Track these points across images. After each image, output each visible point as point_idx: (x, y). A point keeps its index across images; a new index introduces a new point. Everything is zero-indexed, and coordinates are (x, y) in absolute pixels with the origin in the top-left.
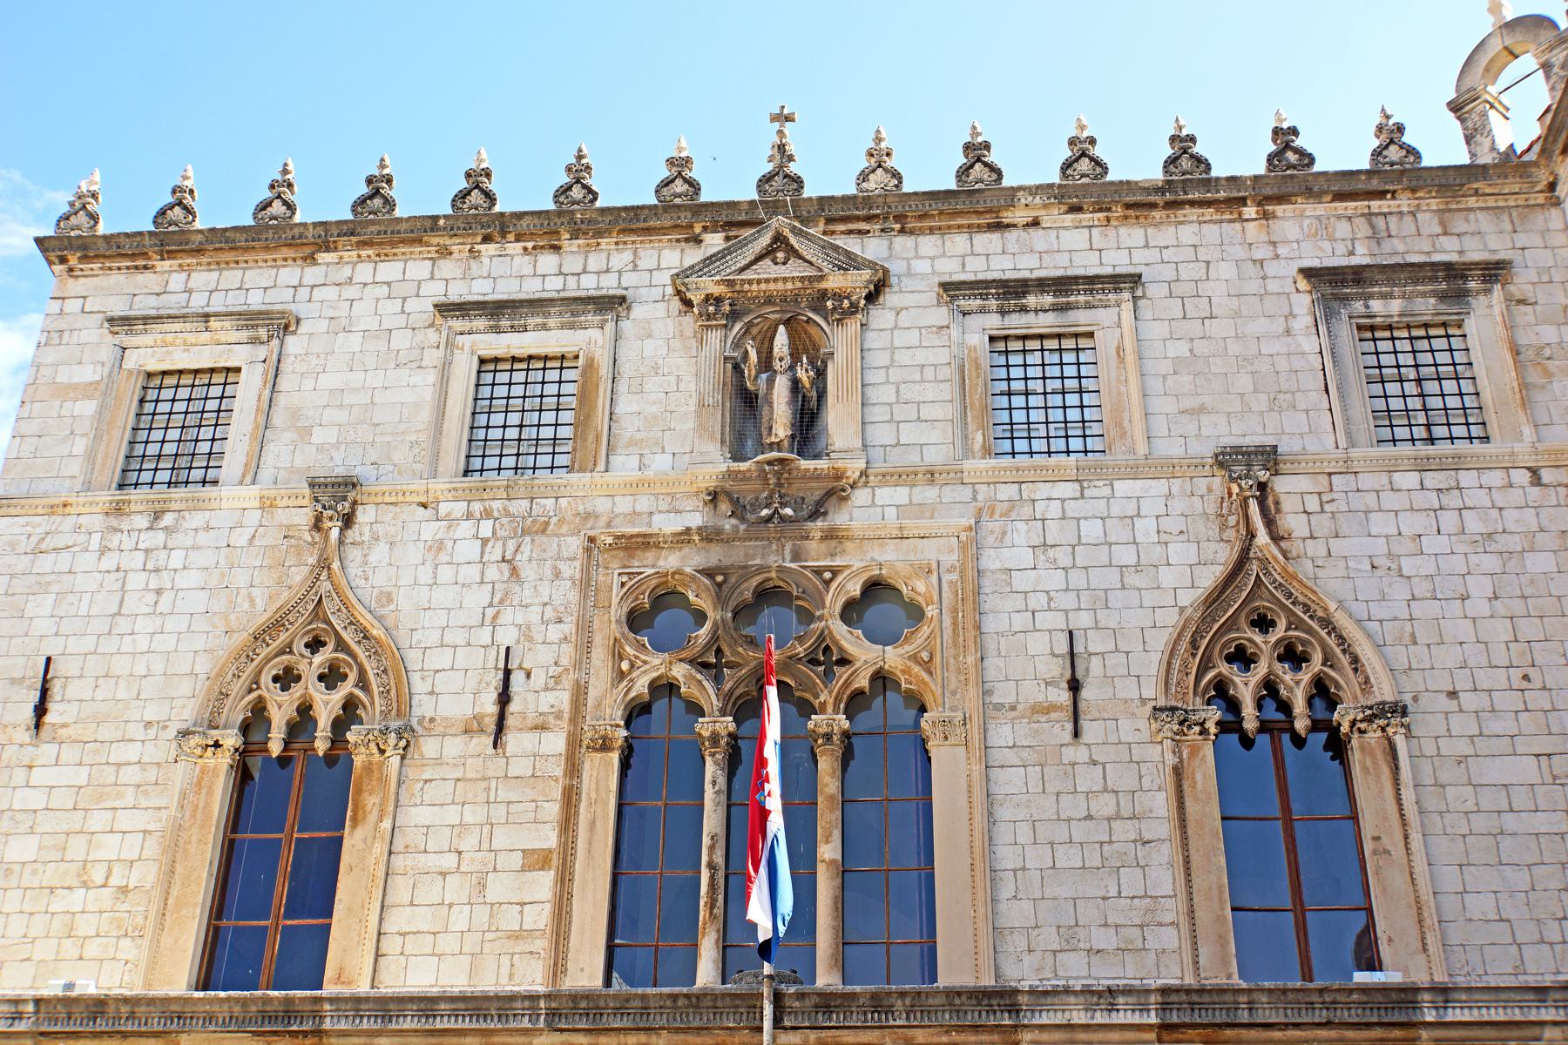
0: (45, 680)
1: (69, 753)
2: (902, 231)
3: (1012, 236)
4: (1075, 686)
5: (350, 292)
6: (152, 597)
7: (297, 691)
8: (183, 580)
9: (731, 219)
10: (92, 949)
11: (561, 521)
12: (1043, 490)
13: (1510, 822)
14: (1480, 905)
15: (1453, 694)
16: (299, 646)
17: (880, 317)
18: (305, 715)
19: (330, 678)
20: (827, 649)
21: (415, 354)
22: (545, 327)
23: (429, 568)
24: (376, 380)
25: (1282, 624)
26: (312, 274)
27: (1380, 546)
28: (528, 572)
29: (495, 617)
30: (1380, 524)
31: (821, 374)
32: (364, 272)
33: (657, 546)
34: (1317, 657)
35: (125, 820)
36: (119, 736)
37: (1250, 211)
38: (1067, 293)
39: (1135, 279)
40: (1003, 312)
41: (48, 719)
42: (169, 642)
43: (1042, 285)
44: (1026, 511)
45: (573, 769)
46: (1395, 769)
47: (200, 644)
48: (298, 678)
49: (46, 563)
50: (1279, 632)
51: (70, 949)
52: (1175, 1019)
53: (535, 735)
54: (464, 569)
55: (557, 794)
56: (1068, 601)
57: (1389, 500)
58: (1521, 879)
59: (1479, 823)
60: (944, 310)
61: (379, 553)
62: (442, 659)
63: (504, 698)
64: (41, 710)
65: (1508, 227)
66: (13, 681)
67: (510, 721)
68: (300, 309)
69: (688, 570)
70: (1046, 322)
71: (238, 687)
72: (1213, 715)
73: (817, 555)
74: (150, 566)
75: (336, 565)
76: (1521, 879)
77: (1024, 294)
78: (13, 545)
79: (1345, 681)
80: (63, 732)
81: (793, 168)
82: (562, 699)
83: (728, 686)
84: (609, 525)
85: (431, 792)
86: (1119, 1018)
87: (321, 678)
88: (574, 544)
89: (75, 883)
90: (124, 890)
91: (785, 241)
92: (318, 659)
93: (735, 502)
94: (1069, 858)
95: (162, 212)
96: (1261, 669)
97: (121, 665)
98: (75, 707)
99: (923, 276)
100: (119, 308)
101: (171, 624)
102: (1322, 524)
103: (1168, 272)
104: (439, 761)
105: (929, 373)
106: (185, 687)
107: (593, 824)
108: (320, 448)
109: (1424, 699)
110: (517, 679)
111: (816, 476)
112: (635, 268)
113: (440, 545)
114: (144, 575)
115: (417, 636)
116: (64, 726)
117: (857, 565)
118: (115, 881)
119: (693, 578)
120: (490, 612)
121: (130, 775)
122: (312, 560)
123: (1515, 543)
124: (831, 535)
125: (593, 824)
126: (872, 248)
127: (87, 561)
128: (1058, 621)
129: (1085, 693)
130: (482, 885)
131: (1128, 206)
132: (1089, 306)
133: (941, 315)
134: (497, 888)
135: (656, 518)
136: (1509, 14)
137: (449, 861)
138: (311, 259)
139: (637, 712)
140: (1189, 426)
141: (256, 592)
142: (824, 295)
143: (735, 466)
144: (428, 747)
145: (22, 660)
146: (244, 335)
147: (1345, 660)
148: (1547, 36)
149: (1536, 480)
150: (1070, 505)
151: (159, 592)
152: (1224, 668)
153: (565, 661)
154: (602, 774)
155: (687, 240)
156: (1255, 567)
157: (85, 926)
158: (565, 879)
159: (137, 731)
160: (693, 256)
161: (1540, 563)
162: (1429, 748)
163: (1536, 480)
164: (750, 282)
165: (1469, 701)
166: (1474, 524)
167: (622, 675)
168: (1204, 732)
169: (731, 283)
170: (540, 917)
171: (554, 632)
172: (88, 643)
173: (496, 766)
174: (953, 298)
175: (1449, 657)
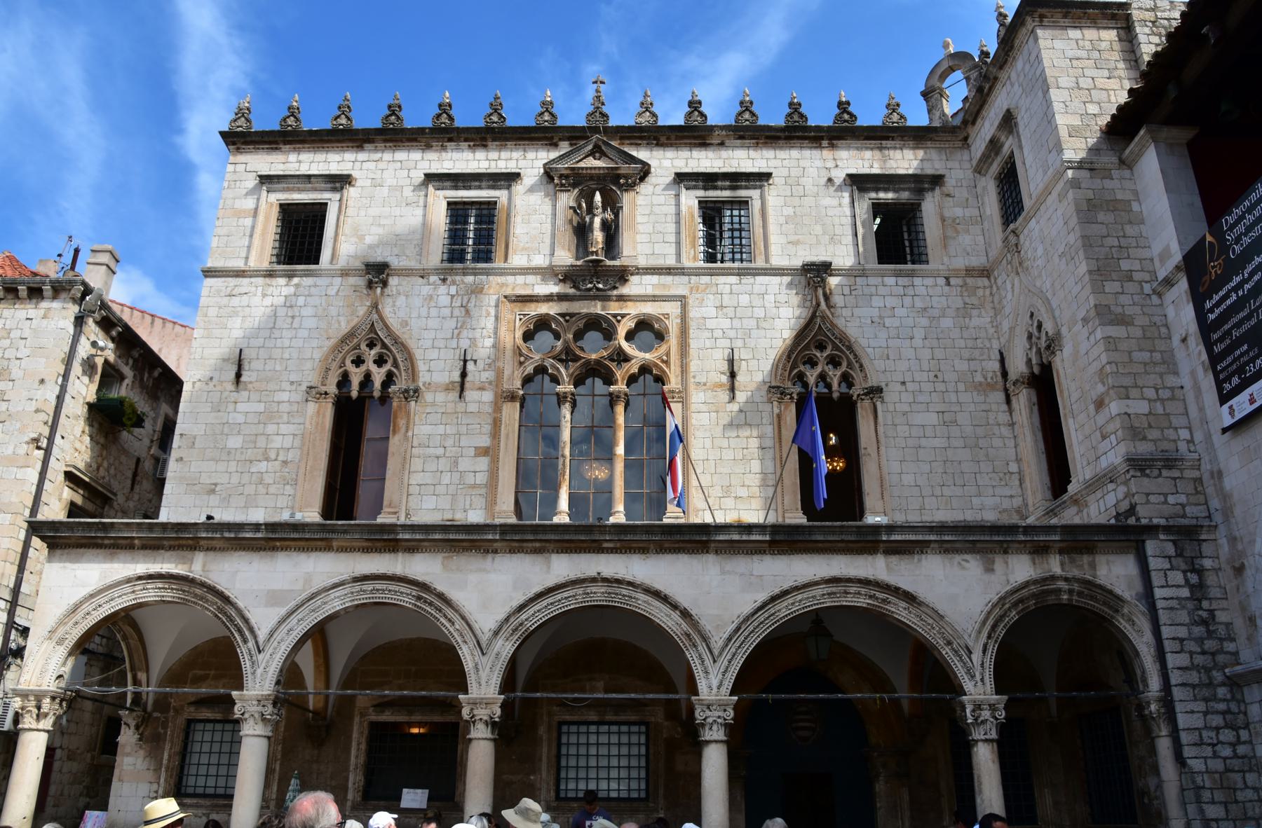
0: (240, 360)
1: (254, 396)
2: (657, 145)
4: (733, 375)
5: (381, 165)
6: (289, 320)
7: (363, 368)
8: (305, 312)
9: (575, 135)
10: (272, 490)
12: (722, 279)
13: (924, 442)
14: (908, 479)
15: (903, 383)
16: (363, 346)
17: (644, 188)
18: (368, 377)
19: (380, 361)
22: (480, 188)
23: (425, 309)
24: (397, 211)
25: (830, 347)
26: (362, 156)
27: (875, 313)
30: (877, 302)
31: (617, 215)
32: (387, 156)
33: (537, 301)
34: (845, 364)
35: (284, 429)
37: (825, 143)
38: (737, 181)
39: (768, 176)
40: (705, 189)
41: (243, 379)
42: (299, 343)
43: (726, 176)
44: (714, 289)
45: (497, 409)
46: (876, 417)
47: (315, 343)
48: (363, 362)
49: (235, 301)
50: (827, 352)
51: (262, 489)
52: (777, 538)
53: (479, 393)
55: (490, 421)
56: (732, 334)
57: (882, 290)
58: (926, 468)
59: (911, 442)
61: (401, 301)
62: (433, 354)
63: (464, 375)
64: (238, 375)
65: (944, 157)
67: (467, 385)
68: (355, 174)
71: (334, 365)
72: (798, 389)
73: (614, 308)
76: (926, 468)
77: (716, 180)
78: (219, 291)
79: (857, 376)
80: (250, 386)
81: (605, 109)
83: (571, 371)
85: (431, 418)
86: (753, 538)
87: (375, 362)
89: (260, 457)
90: (285, 462)
91: (600, 147)
92: (373, 352)
93: (574, 282)
94: (728, 455)
95: (285, 120)
96: (819, 369)
97: (277, 353)
99: (667, 168)
100: (265, 171)
102: (851, 300)
103: (785, 172)
104: (433, 404)
106: (309, 365)
107: (507, 435)
109: (891, 385)
110: (470, 366)
113: (431, 297)
115: (421, 343)
118: (280, 458)
119: (554, 318)
120: (456, 332)
121: (285, 407)
122: (368, 304)
123: (936, 313)
124: (622, 298)
125: (507, 435)
126: (642, 154)
127: (256, 300)
128: (727, 343)
129: (738, 378)
130: (456, 463)
131: (767, 137)
132: (747, 188)
134: (464, 464)
136: (952, 50)
138: (360, 147)
139: (527, 380)
140: (792, 249)
141: (341, 318)
142: (619, 176)
144: (428, 397)
146: (329, 186)
147: (857, 365)
148: (969, 64)
149: (948, 284)
150: (734, 287)
151: (293, 317)
152: (802, 368)
154: (511, 413)
156: (819, 320)
157: (268, 479)
158: (495, 462)
159: (286, 386)
160: (554, 154)
161: (947, 323)
162: (891, 408)
163: (948, 284)
165: (910, 386)
166: (919, 303)
167: (521, 363)
168: (792, 398)
169: (573, 169)
170: (481, 478)
173: (461, 407)
174: (681, 181)
175: (903, 365)
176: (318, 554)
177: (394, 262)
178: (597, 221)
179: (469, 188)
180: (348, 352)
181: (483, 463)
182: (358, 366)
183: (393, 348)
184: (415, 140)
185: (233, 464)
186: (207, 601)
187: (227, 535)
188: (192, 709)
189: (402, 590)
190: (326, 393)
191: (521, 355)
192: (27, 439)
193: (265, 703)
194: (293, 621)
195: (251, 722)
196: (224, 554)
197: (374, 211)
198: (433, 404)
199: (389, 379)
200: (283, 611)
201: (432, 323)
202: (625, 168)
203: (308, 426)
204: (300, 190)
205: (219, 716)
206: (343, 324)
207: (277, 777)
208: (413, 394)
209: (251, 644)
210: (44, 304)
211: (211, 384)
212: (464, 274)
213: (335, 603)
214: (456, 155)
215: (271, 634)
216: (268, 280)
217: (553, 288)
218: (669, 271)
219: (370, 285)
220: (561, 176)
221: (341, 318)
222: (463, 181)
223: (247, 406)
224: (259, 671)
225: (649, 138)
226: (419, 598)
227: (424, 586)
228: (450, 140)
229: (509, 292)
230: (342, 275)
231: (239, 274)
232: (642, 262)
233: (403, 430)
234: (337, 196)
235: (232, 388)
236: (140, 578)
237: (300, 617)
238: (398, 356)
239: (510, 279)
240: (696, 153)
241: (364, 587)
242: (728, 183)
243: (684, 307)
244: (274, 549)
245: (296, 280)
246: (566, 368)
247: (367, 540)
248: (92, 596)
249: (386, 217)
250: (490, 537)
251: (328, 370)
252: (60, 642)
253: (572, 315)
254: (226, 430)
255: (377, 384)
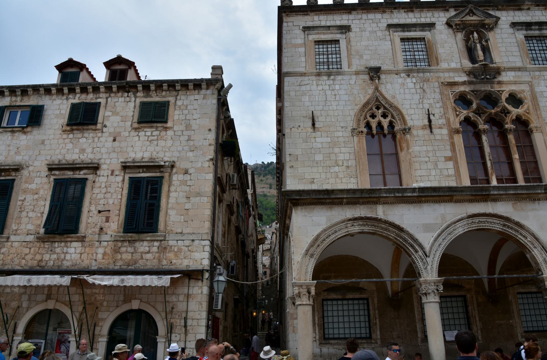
0: (313, 116)
1: (324, 134)
3: (524, 12)
5: (362, 21)
6: (334, 97)
7: (376, 119)
11: (432, 79)
16: (374, 109)
17: (497, 31)
18: (380, 124)
20: (504, 110)
21: (384, 37)
22: (415, 31)
26: (351, 17)
28: (428, 91)
29: (422, 102)
32: (364, 16)
33: (458, 85)
35: (343, 150)
36: (335, 130)
40: (526, 30)
41: (316, 126)
44: (543, 78)
45: (451, 138)
47: (350, 107)
48: (376, 116)
49: (303, 88)
54: (411, 90)
60: (512, 29)
61: (389, 86)
62: (412, 112)
63: (430, 121)
64: (313, 124)
66: (304, 117)
67: (433, 126)
69: (467, 90)
70: (537, 33)
71: (362, 118)
73: (497, 88)
74: (331, 89)
75: (380, 89)
77: (531, 26)
82: (443, 121)
84: (444, 79)
87: (382, 116)
88: (436, 84)
92: (380, 111)
97: (331, 113)
98: (322, 123)
101: (341, 103)
105: (512, 45)
106: (349, 118)
108: (366, 60)
110: (432, 117)
111: (493, 68)
112: (434, 17)
114: (330, 91)
115: (404, 106)
116: (321, 128)
117: (507, 90)
118: (345, 164)
119: (468, 93)
120: (421, 100)
124: (500, 83)
133: (511, 31)
134: (441, 165)
135: (455, 78)
137: (427, 159)
138: (350, 13)
141: (360, 95)
143: (474, 66)
144: (414, 132)
145: (305, 112)
146: (339, 31)
151: (335, 95)
153: (442, 112)
154: (459, 139)
155: (445, 10)
157: (341, 175)
158: (456, 163)
159: (339, 129)
164: (467, 21)
167: (457, 115)
169: (462, 21)
171: (438, 105)
172: (321, 108)
173: (432, 137)
174: (515, 26)
176: (445, 204)
177: (384, 68)
178: (478, 46)
179: (410, 31)
180: (367, 112)
181: (450, 164)
182: (373, 118)
183: (390, 109)
184: (377, 9)
185: (321, 168)
186: (389, 231)
187: (397, 195)
188: (325, 294)
189: (495, 221)
190: (362, 132)
191: (456, 111)
192: (207, 159)
193: (438, 284)
194: (440, 239)
195: (432, 295)
196: (393, 205)
197: (364, 43)
198: (418, 136)
199: (391, 125)
200: (435, 235)
201: (407, 96)
202: (487, 21)
203: (356, 148)
204: (324, 34)
205: (340, 297)
206: (362, 98)
207: (378, 327)
208: (407, 131)
209: (420, 253)
210: (203, 92)
211: (300, 129)
212: (418, 72)
213: (460, 230)
214: (399, 15)
215: (431, 248)
216: (318, 78)
217: (464, 78)
218: (519, 69)
219: (372, 79)
220: (456, 25)
221: (360, 95)
222: (407, 28)
223: (321, 140)
224: (429, 267)
225: (493, 6)
226: (504, 225)
227: (507, 219)
228: (395, 8)
229: (442, 80)
230: (356, 74)
231: (303, 74)
232: (505, 65)
233: (406, 149)
234: (344, 36)
235: (310, 130)
236: (350, 220)
237: (443, 237)
238: (394, 113)
239: (441, 75)
240: (517, 13)
241: (474, 221)
242: (537, 27)
243: (531, 86)
244: (420, 202)
245: (332, 77)
246: (480, 116)
247: (472, 195)
248: (325, 230)
249: (370, 46)
250: (539, 191)
251: (359, 120)
252: (312, 256)
253: (477, 91)
254: (313, 152)
255: (386, 127)
